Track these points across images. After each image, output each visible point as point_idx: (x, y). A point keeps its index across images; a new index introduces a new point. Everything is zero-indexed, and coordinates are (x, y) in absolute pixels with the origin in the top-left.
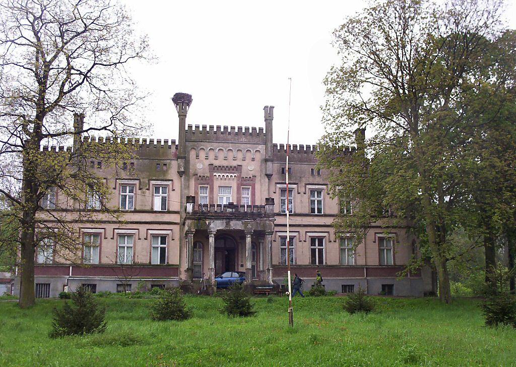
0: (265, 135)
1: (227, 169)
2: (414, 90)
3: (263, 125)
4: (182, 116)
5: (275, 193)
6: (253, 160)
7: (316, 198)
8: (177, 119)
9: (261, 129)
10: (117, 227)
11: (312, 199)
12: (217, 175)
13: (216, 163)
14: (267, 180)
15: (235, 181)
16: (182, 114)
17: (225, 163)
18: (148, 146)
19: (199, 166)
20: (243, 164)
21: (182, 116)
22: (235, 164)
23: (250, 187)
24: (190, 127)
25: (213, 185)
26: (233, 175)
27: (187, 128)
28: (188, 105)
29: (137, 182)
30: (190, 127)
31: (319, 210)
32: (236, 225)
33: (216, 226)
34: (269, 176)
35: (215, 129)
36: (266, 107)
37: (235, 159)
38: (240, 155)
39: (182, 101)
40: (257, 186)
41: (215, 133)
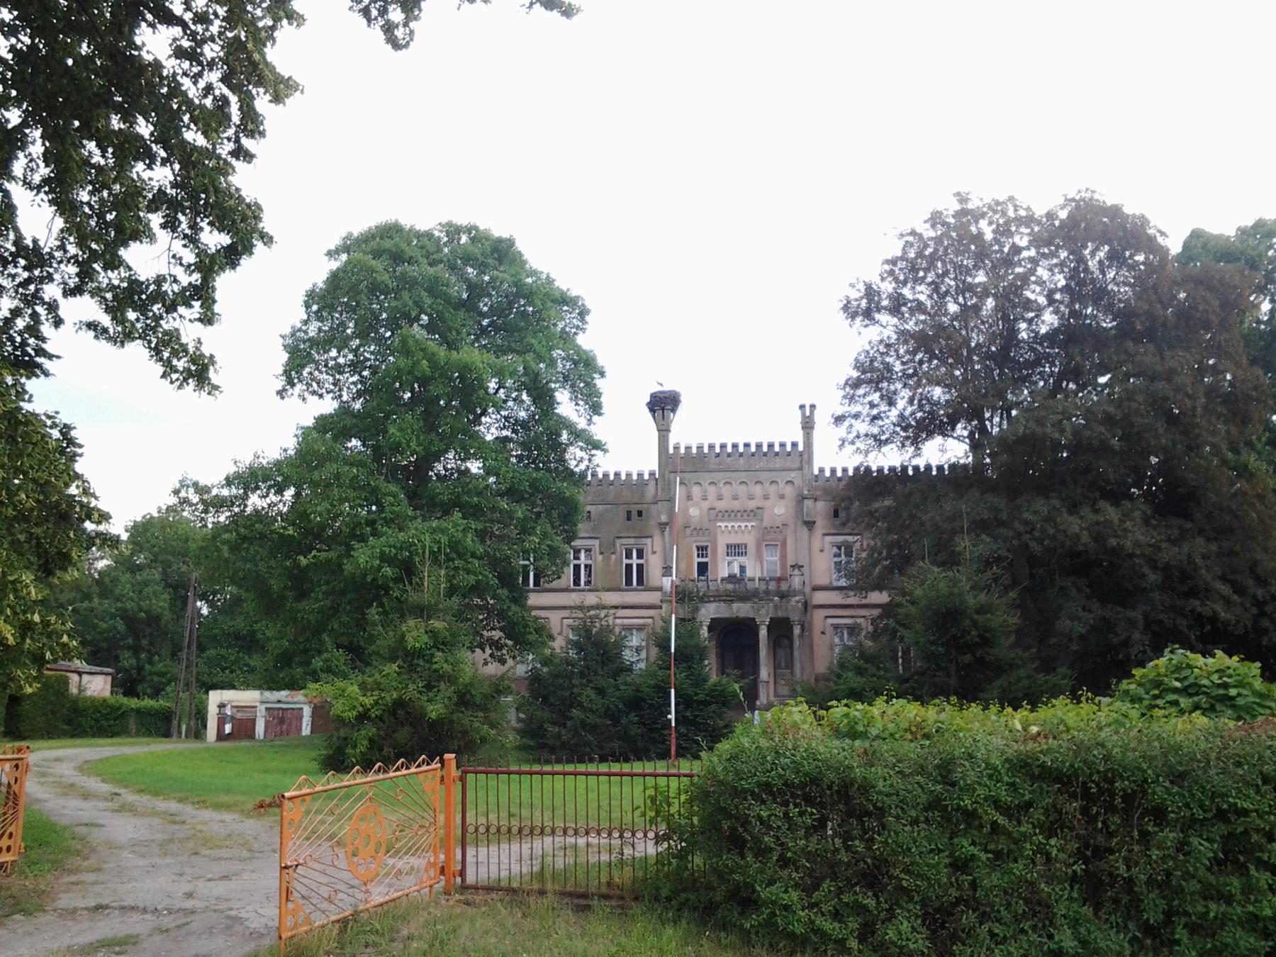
0: (801, 454)
1: (739, 514)
2: (136, 297)
3: (799, 437)
4: (664, 431)
5: (822, 551)
6: (782, 497)
7: (635, 561)
8: (656, 434)
9: (794, 445)
10: (567, 615)
11: (640, 561)
12: (723, 525)
13: (721, 505)
14: (805, 530)
15: (752, 534)
16: (663, 428)
17: (736, 505)
18: (612, 484)
19: (694, 512)
20: (767, 504)
21: (664, 431)
22: (752, 505)
23: (779, 543)
24: (676, 448)
25: (715, 541)
26: (749, 525)
27: (671, 451)
28: (673, 410)
29: (596, 542)
30: (676, 448)
31: (588, 583)
32: (741, 610)
33: (709, 612)
34: (810, 525)
35: (718, 450)
36: (802, 407)
37: (751, 498)
38: (757, 490)
39: (662, 405)
40: (790, 542)
41: (718, 455)
